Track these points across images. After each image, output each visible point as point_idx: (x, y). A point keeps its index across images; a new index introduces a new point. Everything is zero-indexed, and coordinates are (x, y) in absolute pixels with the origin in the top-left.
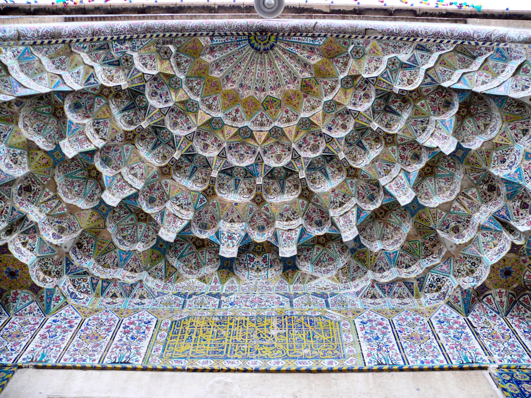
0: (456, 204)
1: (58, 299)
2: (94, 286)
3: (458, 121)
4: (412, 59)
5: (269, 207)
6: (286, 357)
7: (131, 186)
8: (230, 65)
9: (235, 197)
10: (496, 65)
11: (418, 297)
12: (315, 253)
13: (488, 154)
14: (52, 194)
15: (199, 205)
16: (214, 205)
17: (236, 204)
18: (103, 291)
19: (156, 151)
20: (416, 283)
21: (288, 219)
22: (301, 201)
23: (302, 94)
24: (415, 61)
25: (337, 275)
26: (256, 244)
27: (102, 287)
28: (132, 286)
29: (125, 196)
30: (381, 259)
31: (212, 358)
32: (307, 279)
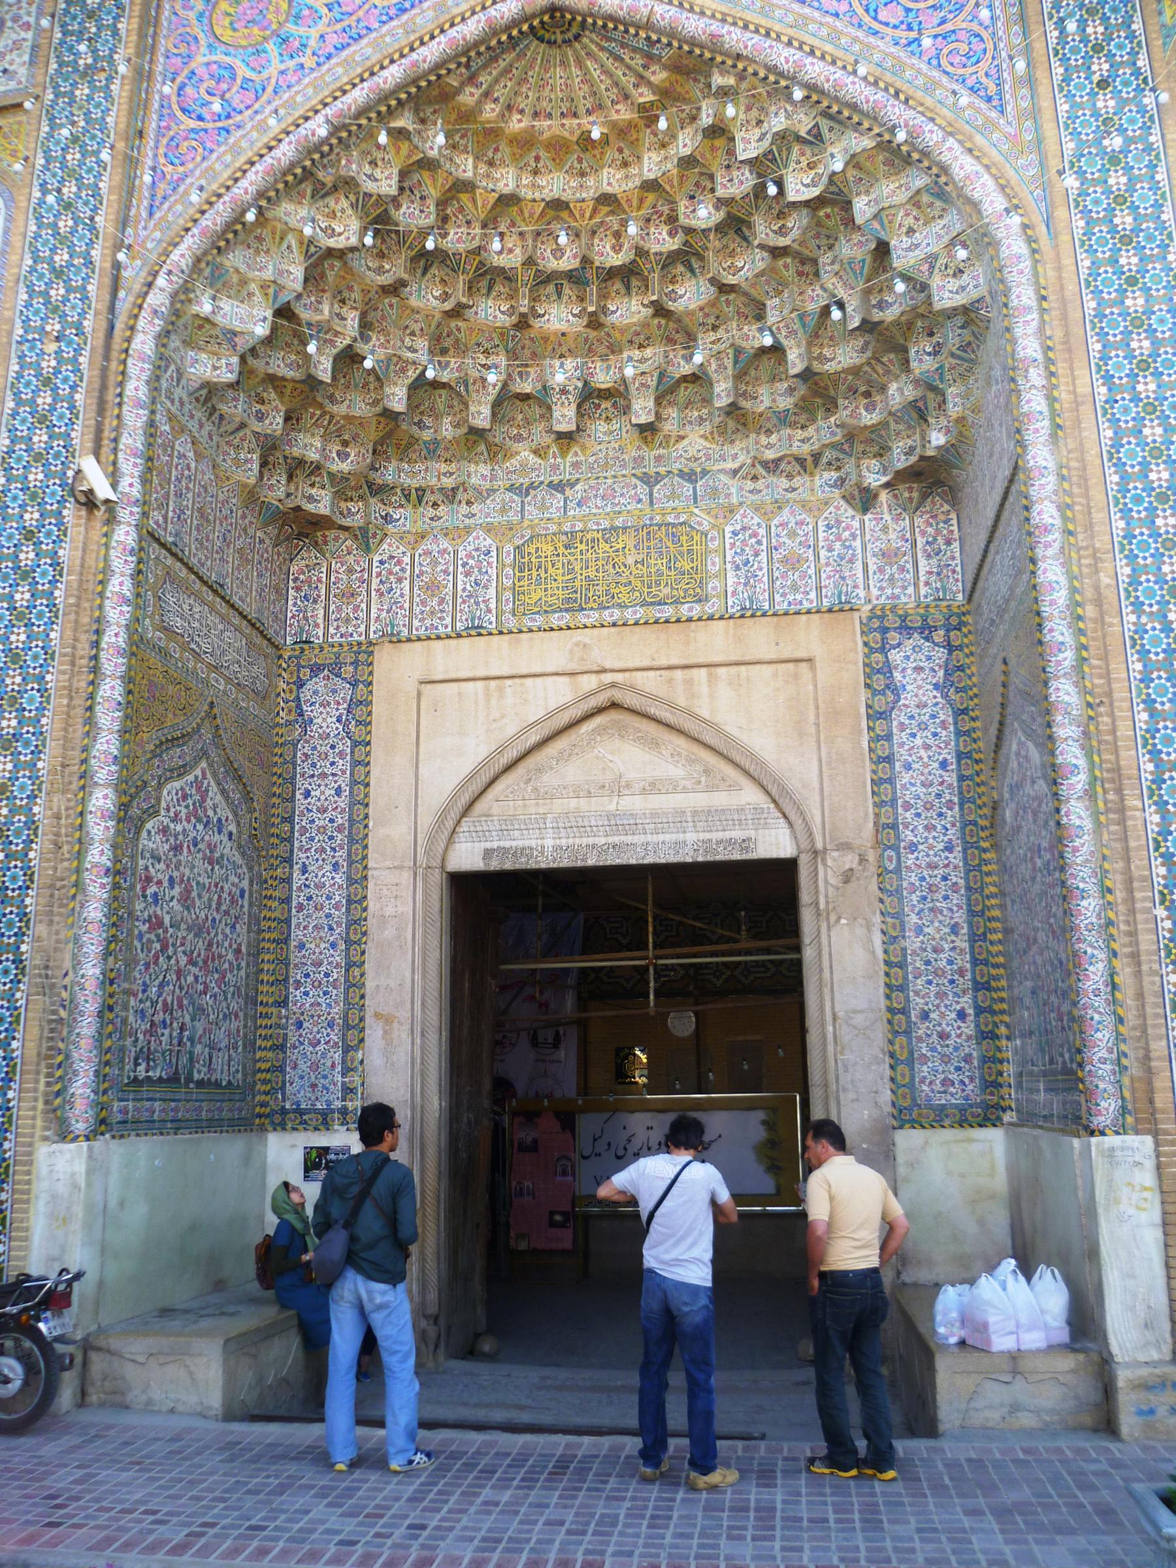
0: (867, 368)
1: (375, 535)
2: (407, 497)
3: (875, 260)
4: (815, 131)
5: (612, 332)
6: (645, 604)
7: (414, 363)
8: (509, 84)
9: (559, 316)
10: (932, 204)
11: (812, 474)
12: (683, 393)
13: (910, 325)
14: (318, 412)
15: (511, 345)
16: (532, 339)
17: (563, 334)
18: (420, 502)
19: (428, 276)
20: (810, 459)
21: (641, 346)
22: (656, 321)
23: (641, 123)
24: (819, 136)
25: (712, 433)
26: (600, 390)
28: (454, 490)
29: (410, 380)
30: (768, 419)
31: (567, 610)
32: (673, 440)
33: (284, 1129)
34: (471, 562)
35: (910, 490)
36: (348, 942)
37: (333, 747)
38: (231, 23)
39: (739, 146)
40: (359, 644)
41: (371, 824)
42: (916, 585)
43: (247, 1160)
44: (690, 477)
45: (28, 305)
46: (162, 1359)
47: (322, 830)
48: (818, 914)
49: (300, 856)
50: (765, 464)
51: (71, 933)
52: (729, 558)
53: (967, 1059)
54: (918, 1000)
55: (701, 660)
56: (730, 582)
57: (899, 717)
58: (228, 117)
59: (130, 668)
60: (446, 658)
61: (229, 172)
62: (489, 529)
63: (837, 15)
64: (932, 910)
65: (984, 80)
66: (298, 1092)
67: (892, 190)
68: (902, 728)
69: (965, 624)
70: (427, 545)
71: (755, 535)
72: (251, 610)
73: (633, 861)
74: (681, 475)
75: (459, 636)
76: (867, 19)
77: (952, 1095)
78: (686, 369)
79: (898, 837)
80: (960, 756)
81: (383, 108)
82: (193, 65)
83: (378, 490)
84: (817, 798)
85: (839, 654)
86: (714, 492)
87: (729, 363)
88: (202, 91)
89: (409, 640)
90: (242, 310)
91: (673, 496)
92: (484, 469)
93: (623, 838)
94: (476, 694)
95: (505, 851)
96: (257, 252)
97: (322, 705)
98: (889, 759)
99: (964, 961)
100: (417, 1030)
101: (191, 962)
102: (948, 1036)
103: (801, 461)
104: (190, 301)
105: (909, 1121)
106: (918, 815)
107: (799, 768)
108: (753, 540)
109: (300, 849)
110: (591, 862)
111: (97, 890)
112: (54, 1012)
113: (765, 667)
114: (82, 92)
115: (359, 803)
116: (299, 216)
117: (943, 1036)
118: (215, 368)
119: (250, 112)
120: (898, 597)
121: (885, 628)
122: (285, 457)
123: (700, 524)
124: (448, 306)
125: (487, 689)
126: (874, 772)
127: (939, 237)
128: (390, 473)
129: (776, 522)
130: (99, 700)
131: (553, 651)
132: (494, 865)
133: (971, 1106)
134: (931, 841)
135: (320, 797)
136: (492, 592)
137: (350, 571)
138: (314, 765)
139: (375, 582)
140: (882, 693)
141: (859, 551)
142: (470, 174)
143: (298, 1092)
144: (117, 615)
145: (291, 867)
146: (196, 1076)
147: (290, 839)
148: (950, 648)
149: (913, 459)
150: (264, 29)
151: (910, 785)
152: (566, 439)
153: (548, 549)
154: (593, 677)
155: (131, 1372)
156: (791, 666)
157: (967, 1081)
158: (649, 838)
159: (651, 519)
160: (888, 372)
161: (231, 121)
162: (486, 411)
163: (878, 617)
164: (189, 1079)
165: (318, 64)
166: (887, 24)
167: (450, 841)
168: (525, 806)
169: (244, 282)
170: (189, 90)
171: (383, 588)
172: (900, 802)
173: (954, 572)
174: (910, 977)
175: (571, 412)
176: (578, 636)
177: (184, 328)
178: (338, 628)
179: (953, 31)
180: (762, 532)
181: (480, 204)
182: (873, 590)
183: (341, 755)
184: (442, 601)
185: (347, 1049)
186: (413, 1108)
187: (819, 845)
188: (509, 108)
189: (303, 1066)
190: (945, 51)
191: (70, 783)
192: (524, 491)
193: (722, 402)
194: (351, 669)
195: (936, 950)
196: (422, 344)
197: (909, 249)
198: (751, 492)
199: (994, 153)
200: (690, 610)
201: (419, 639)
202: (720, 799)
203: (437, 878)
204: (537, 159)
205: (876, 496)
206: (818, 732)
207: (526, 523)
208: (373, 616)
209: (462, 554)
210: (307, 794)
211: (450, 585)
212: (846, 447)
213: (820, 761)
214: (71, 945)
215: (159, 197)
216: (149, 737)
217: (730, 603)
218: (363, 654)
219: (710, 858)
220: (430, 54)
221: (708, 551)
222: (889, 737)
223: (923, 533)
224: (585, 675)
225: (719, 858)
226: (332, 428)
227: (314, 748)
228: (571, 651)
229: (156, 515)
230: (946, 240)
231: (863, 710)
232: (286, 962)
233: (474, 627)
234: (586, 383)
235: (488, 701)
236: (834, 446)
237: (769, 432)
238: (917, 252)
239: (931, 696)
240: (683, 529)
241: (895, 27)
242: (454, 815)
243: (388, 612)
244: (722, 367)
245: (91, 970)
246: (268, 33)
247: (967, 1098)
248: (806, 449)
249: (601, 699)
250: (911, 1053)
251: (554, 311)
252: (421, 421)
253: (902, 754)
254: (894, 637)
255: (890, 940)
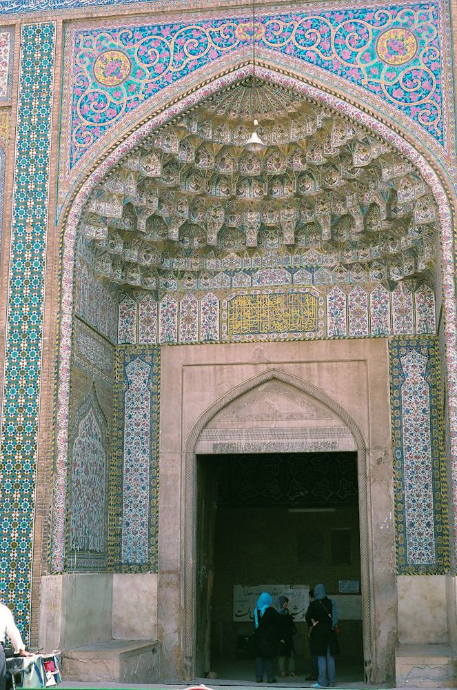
4: (365, 140)
11: (368, 271)
18: (182, 277)
22: (295, 199)
27: (181, 275)
31: (252, 333)
33: (121, 572)
34: (207, 307)
35: (413, 282)
36: (150, 486)
37: (142, 395)
38: (103, 73)
39: (333, 140)
40: (154, 345)
41: (160, 432)
42: (415, 326)
43: (107, 586)
44: (311, 269)
45: (17, 209)
46: (94, 661)
47: (137, 434)
48: (366, 477)
49: (127, 447)
50: (346, 266)
51: (51, 490)
52: (328, 311)
55: (315, 359)
56: (329, 322)
57: (404, 389)
58: (104, 121)
59: (71, 376)
60: (196, 355)
61: (105, 150)
62: (215, 291)
63: (375, 93)
64: (416, 477)
65: (436, 129)
66: (127, 556)
67: (399, 170)
68: (406, 393)
69: (437, 345)
70: (186, 298)
71: (341, 300)
72: (105, 334)
73: (282, 451)
74: (307, 268)
75: (202, 343)
76: (388, 95)
78: (310, 219)
79: (402, 443)
80: (431, 407)
81: (174, 121)
82: (86, 92)
83: (162, 272)
84: (367, 425)
85: (378, 359)
86: (322, 279)
87: (329, 221)
88: (91, 106)
89: (178, 344)
90: (109, 207)
91: (303, 279)
92: (213, 261)
93: (278, 440)
94: (210, 371)
95: (223, 445)
96: (116, 181)
97: (136, 374)
98: (399, 408)
99: (430, 501)
100: (183, 527)
101: (88, 498)
102: (422, 534)
103: (363, 265)
104: (88, 207)
105: (404, 572)
106: (412, 434)
107: (360, 411)
108: (340, 302)
109: (127, 443)
110: (263, 451)
111: (62, 472)
112: (46, 522)
113: (344, 363)
114: (35, 103)
115: (155, 422)
116: (135, 164)
117: (420, 534)
118: (97, 233)
119: (114, 119)
120: (406, 332)
121: (400, 346)
122: (122, 262)
123: (315, 293)
124: (198, 192)
125: (215, 369)
126: (392, 414)
127: (418, 193)
128: (167, 264)
129: (350, 294)
130: (59, 391)
131: (246, 353)
132: (218, 452)
133: (431, 565)
134: (417, 446)
135: (136, 418)
136: (217, 323)
137: (148, 309)
138: (133, 403)
139: (161, 316)
140: (397, 377)
141: (389, 309)
142: (211, 137)
143: (127, 556)
144: (65, 355)
145: (123, 451)
146: (90, 548)
147: (122, 438)
148: (429, 356)
149: (412, 272)
150: (119, 78)
151: (409, 420)
152: (252, 250)
153: (243, 303)
154: (265, 366)
155: (80, 666)
156: (356, 363)
158: (290, 441)
159: (292, 290)
160: (401, 233)
161: (106, 124)
162: (215, 237)
163: (396, 341)
164: (88, 549)
165: (145, 99)
166: (396, 99)
167: (197, 440)
168: (232, 424)
169: (111, 195)
170: (85, 106)
171: (165, 319)
172: (404, 428)
173: (432, 320)
175: (255, 237)
176: (258, 346)
177: (87, 218)
178: (143, 337)
179: (425, 104)
180: (344, 298)
181: (214, 149)
182: (394, 326)
183: (146, 399)
184: (193, 326)
185: (150, 536)
186: (181, 563)
187: (367, 447)
188: (229, 110)
189: (130, 543)
190: (421, 114)
191: (49, 427)
192: (232, 273)
193: (326, 238)
194: (150, 357)
195: (418, 496)
196: (186, 209)
197: (405, 196)
198: (339, 278)
199: (438, 164)
200: (310, 335)
201: (182, 344)
202: (323, 423)
203: (192, 457)
204: (241, 128)
205: (397, 284)
206: (368, 394)
207: (233, 290)
208: (160, 332)
209: (202, 303)
210: (130, 417)
211: (197, 319)
212: (383, 261)
213: (368, 408)
214: (52, 495)
215: (74, 158)
216: (76, 401)
217: (329, 332)
218: (155, 350)
219: (317, 451)
220: (196, 97)
221: (319, 307)
222: (399, 398)
223: (419, 302)
224: (262, 365)
225: (321, 451)
226: (143, 246)
227: (133, 395)
228: (254, 353)
229: (77, 307)
230: (420, 195)
231: (388, 385)
232: (121, 495)
233: (208, 340)
234: (262, 224)
235: (215, 375)
236: (377, 260)
237: (348, 251)
238: (408, 198)
239: (419, 378)
240: (307, 295)
241: (400, 100)
242: (199, 428)
243: (167, 330)
244: (325, 222)
245: (61, 505)
246: (121, 80)
248: (365, 260)
249: (269, 376)
250: (405, 541)
251: (247, 191)
252: (183, 239)
253: (405, 406)
254: (403, 351)
255: (398, 491)
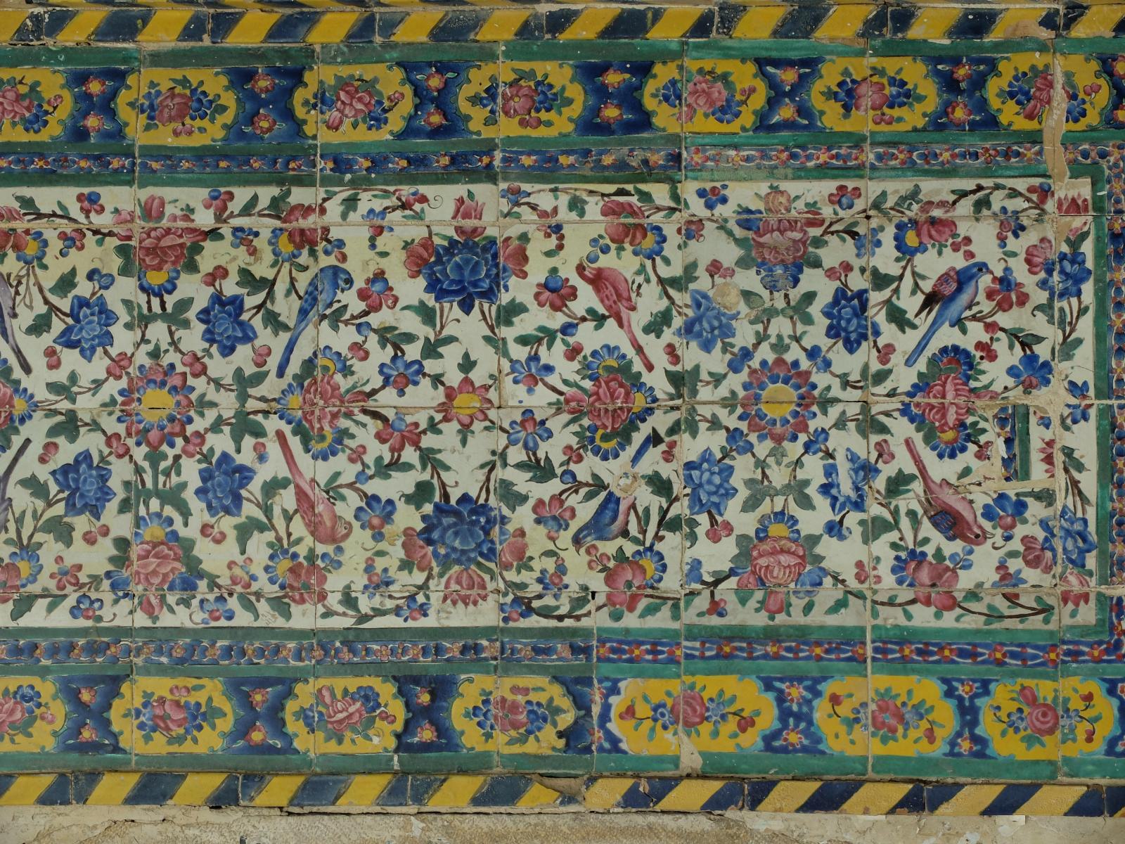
53: (779, 250)
54: (348, 574)
77: (1034, 372)
157: (935, 264)
174: (180, 617)
247: (1066, 271)
250: (727, 647)
